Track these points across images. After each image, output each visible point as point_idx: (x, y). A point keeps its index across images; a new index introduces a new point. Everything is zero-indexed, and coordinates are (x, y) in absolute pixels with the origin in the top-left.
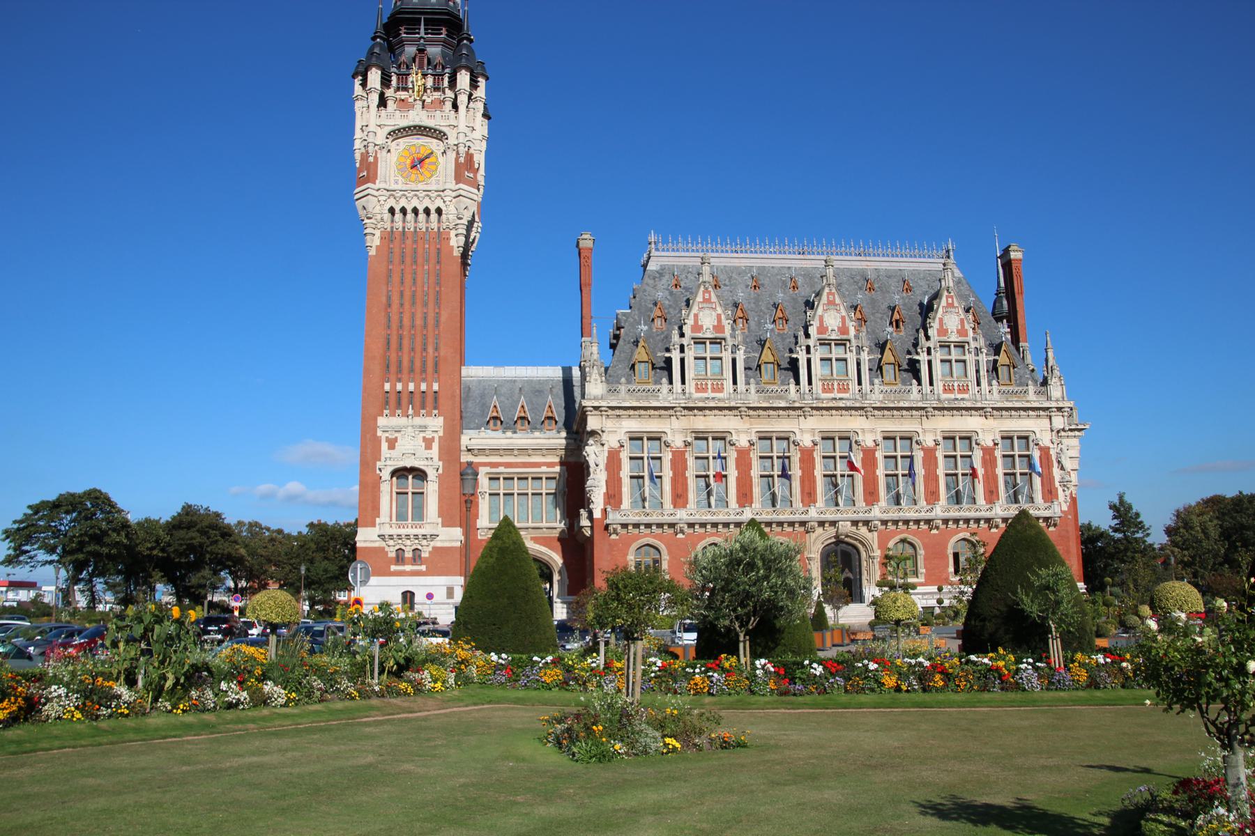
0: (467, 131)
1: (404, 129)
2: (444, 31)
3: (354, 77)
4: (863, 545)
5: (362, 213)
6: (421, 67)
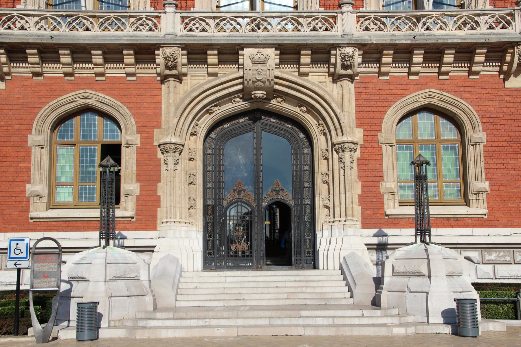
4: (311, 109)
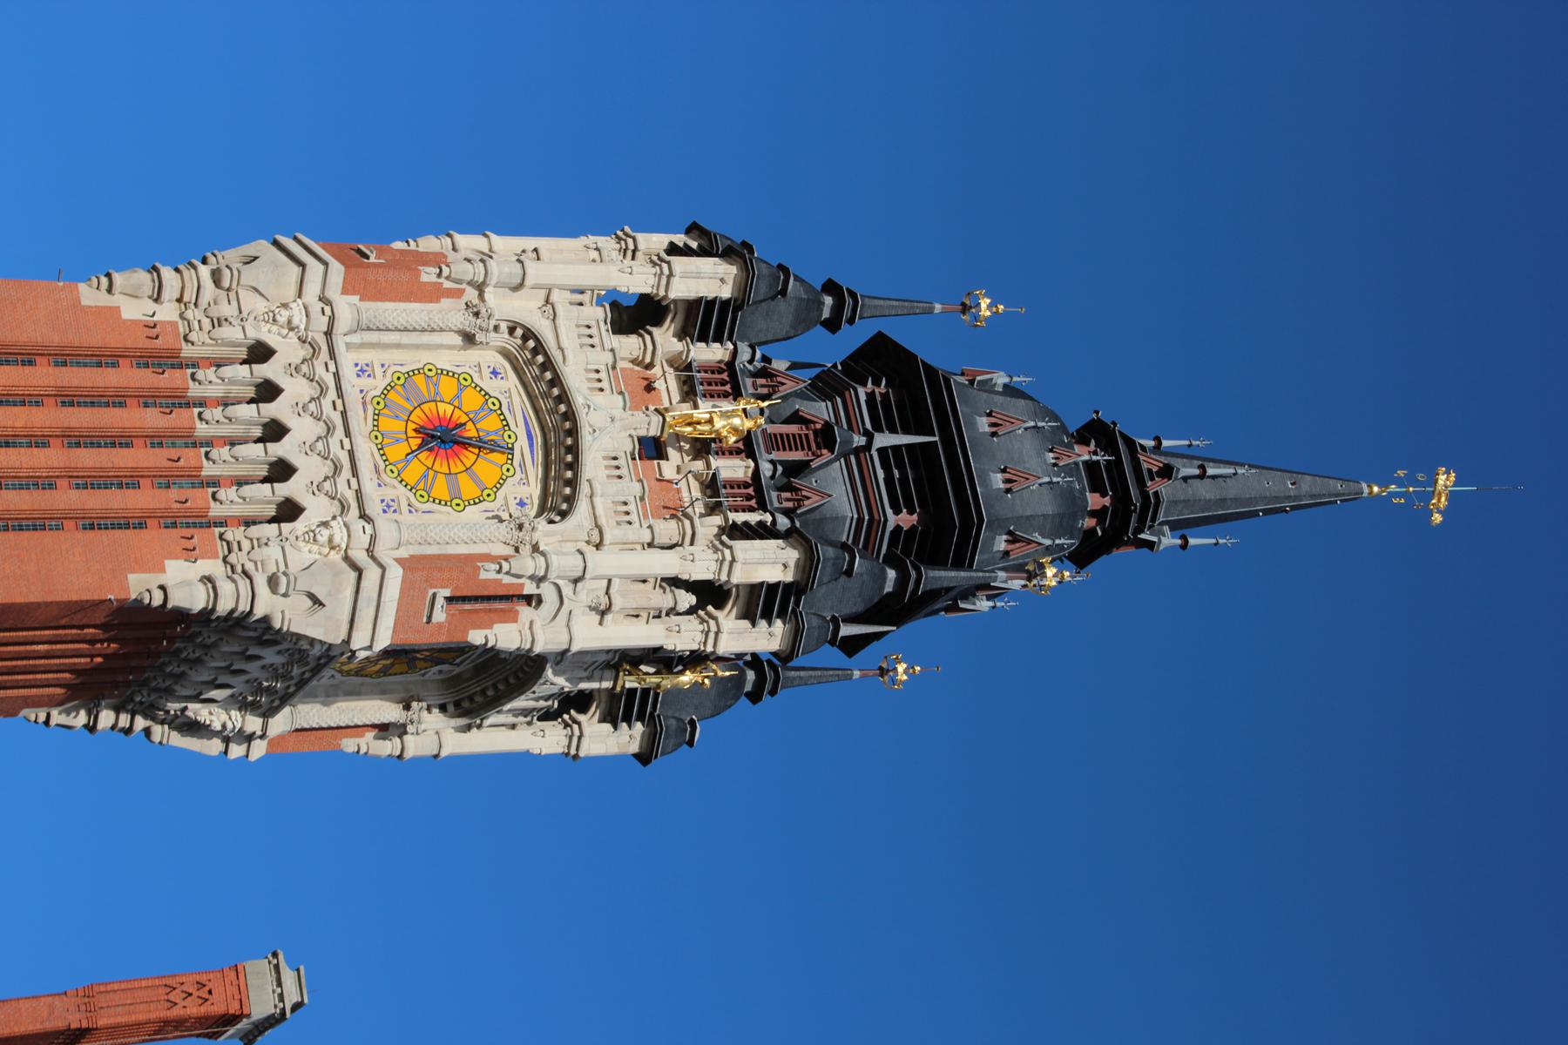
0: (592, 590)
1: (556, 381)
2: (907, 520)
3: (693, 229)
5: (232, 256)
6: (775, 442)
